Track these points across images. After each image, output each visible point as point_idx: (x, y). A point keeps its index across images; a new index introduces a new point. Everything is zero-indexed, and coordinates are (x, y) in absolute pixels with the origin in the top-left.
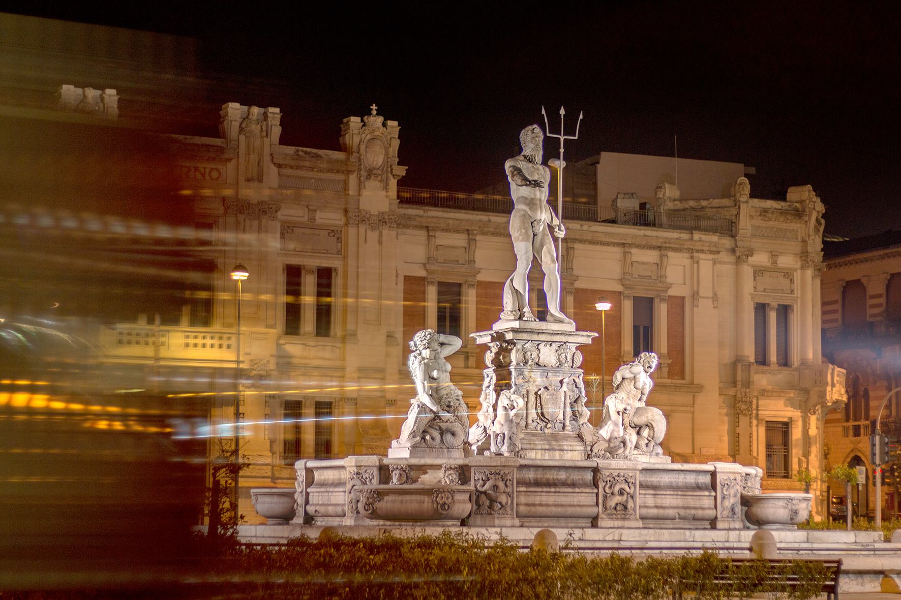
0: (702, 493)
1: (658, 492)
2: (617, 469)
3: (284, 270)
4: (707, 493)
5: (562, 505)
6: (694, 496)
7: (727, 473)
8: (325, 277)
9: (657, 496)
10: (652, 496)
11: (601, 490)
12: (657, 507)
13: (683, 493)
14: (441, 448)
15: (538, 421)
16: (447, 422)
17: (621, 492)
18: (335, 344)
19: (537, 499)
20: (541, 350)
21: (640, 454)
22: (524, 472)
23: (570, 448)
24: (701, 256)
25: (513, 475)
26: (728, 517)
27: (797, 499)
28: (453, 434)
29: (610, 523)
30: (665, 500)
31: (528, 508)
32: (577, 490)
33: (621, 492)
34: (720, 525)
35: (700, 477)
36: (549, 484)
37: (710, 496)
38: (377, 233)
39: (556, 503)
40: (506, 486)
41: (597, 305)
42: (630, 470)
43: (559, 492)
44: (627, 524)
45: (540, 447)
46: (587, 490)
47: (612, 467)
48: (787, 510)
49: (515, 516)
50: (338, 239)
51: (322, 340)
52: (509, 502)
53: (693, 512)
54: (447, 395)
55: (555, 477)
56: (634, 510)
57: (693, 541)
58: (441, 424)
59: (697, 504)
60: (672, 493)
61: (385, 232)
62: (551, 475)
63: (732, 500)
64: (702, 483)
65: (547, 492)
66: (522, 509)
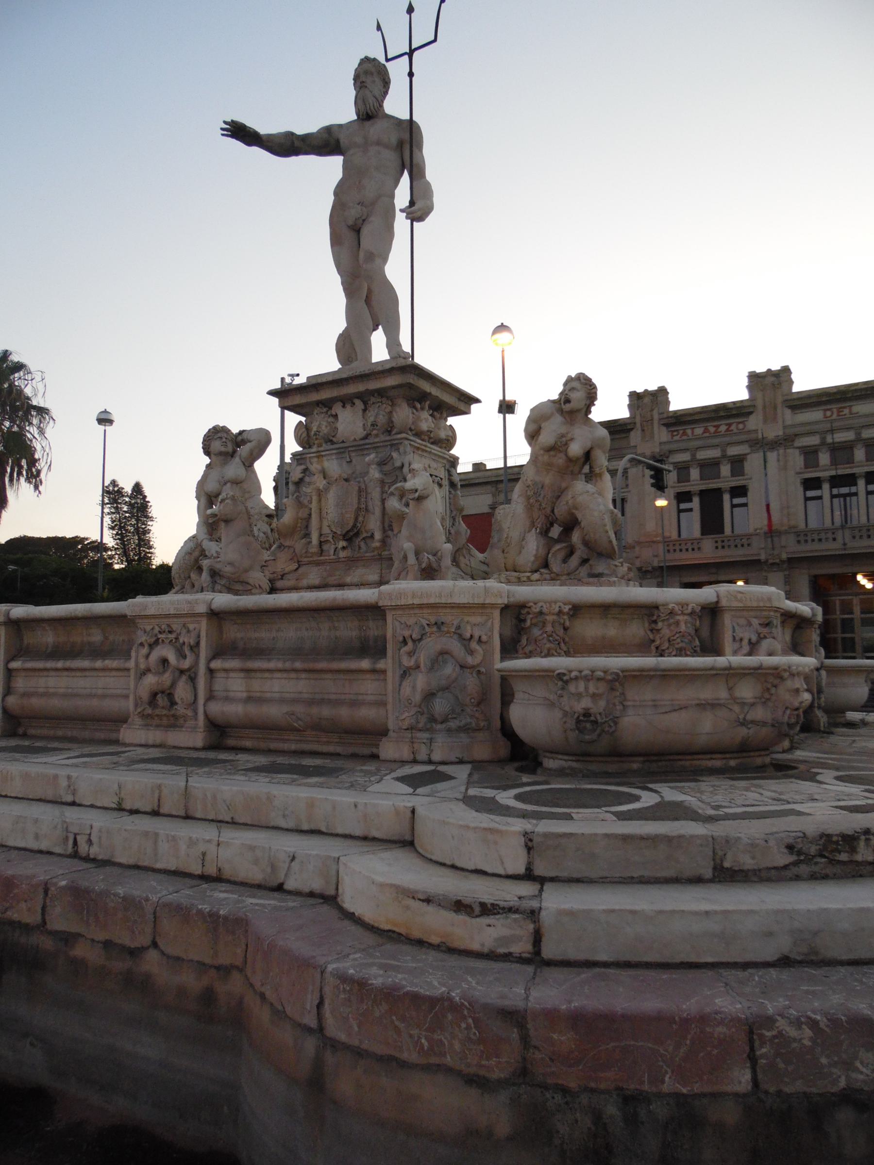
0: (354, 665)
4: (365, 664)
6: (339, 671)
9: (253, 674)
10: (242, 675)
12: (249, 699)
15: (330, 539)
21: (545, 580)
26: (411, 728)
27: (587, 679)
34: (388, 749)
48: (558, 714)
62: (79, 637)
63: (421, 681)
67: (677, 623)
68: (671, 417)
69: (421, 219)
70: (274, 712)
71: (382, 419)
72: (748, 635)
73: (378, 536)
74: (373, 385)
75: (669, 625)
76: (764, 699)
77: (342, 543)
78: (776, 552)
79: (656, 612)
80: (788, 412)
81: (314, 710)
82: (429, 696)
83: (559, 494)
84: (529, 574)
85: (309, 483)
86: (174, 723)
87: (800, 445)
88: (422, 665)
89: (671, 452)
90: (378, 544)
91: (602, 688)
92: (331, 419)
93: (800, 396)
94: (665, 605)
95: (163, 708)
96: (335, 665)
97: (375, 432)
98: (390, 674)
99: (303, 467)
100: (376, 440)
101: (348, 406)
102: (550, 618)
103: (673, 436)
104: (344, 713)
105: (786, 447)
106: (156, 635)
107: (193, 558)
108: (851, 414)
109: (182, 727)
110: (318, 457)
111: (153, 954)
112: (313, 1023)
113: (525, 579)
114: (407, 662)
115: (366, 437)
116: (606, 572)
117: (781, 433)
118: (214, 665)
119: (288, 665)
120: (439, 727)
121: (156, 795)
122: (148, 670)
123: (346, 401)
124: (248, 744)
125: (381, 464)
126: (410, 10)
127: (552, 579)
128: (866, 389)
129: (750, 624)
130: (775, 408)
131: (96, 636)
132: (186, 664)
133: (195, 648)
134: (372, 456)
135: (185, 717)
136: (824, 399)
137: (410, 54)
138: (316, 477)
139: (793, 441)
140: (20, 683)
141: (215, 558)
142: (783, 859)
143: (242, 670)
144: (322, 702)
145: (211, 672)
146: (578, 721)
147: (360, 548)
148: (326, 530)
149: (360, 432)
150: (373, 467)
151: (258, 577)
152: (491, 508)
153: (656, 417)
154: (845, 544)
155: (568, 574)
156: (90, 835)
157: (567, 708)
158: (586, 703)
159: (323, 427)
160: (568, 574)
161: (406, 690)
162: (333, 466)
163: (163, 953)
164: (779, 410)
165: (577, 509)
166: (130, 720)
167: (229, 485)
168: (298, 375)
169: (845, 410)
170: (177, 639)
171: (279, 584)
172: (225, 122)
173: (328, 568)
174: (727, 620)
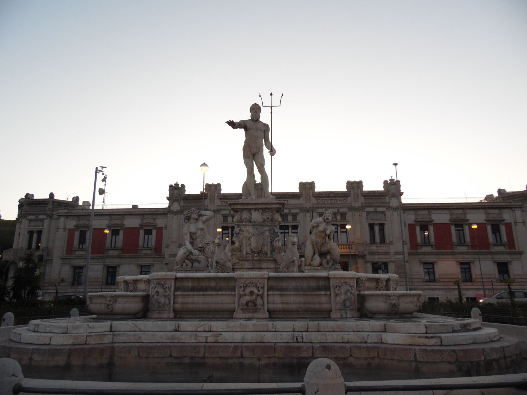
0: (319, 293)
1: (283, 293)
2: (249, 278)
3: (368, 225)
4: (323, 293)
7: (339, 278)
8: (382, 226)
9: (283, 296)
10: (279, 296)
11: (236, 292)
13: (304, 293)
14: (192, 270)
15: (250, 253)
16: (196, 256)
17: (252, 293)
19: (191, 299)
21: (322, 269)
22: (185, 282)
24: (516, 209)
25: (171, 285)
27: (395, 296)
29: (243, 315)
32: (220, 293)
34: (333, 315)
35: (320, 282)
36: (201, 289)
37: (326, 295)
40: (166, 292)
41: (472, 226)
42: (260, 278)
43: (206, 295)
44: (256, 315)
46: (227, 293)
47: (244, 277)
48: (387, 304)
52: (167, 302)
53: (311, 306)
55: (207, 285)
56: (263, 305)
57: (275, 331)
58: (192, 257)
60: (294, 293)
62: (203, 284)
63: (343, 297)
65: (197, 295)
66: (177, 306)
67: (383, 283)
68: (222, 196)
69: (274, 155)
70: (294, 307)
71: (270, 217)
72: (394, 286)
73: (269, 253)
74: (268, 206)
75: (381, 284)
76: (418, 301)
77: (256, 255)
79: (379, 280)
81: (307, 306)
82: (344, 301)
83: (323, 244)
85: (241, 234)
86: (255, 311)
88: (343, 294)
89: (221, 210)
90: (270, 256)
91: (396, 298)
92: (250, 214)
94: (381, 279)
96: (313, 293)
97: (267, 221)
98: (332, 295)
100: (268, 223)
102: (364, 281)
103: (222, 204)
104: (317, 306)
106: (247, 284)
109: (259, 312)
110: (245, 226)
111: (351, 358)
112: (414, 359)
114: (337, 292)
116: (338, 268)
118: (269, 293)
119: (297, 293)
120: (348, 309)
121: (307, 327)
122: (245, 295)
123: (255, 210)
124: (280, 316)
125: (270, 231)
126: (271, 94)
127: (324, 269)
128: (293, 195)
129: (394, 284)
131: (213, 284)
132: (260, 293)
133: (263, 288)
134: (268, 228)
135: (260, 309)
137: (271, 107)
138: (245, 232)
140: (180, 300)
142: (460, 328)
143: (279, 295)
144: (308, 303)
145: (268, 295)
146: (392, 306)
147: (261, 256)
148: (248, 249)
149: (261, 220)
150: (267, 231)
151: (229, 264)
152: (140, 226)
153: (216, 195)
155: (329, 268)
156: (302, 336)
157: (389, 303)
158: (395, 301)
159: (248, 217)
160: (329, 268)
161: (338, 299)
162: (250, 229)
163: (354, 357)
165: (331, 249)
166: (236, 311)
167: (200, 230)
168: (106, 167)
170: (256, 285)
171: (235, 267)
174: (391, 283)
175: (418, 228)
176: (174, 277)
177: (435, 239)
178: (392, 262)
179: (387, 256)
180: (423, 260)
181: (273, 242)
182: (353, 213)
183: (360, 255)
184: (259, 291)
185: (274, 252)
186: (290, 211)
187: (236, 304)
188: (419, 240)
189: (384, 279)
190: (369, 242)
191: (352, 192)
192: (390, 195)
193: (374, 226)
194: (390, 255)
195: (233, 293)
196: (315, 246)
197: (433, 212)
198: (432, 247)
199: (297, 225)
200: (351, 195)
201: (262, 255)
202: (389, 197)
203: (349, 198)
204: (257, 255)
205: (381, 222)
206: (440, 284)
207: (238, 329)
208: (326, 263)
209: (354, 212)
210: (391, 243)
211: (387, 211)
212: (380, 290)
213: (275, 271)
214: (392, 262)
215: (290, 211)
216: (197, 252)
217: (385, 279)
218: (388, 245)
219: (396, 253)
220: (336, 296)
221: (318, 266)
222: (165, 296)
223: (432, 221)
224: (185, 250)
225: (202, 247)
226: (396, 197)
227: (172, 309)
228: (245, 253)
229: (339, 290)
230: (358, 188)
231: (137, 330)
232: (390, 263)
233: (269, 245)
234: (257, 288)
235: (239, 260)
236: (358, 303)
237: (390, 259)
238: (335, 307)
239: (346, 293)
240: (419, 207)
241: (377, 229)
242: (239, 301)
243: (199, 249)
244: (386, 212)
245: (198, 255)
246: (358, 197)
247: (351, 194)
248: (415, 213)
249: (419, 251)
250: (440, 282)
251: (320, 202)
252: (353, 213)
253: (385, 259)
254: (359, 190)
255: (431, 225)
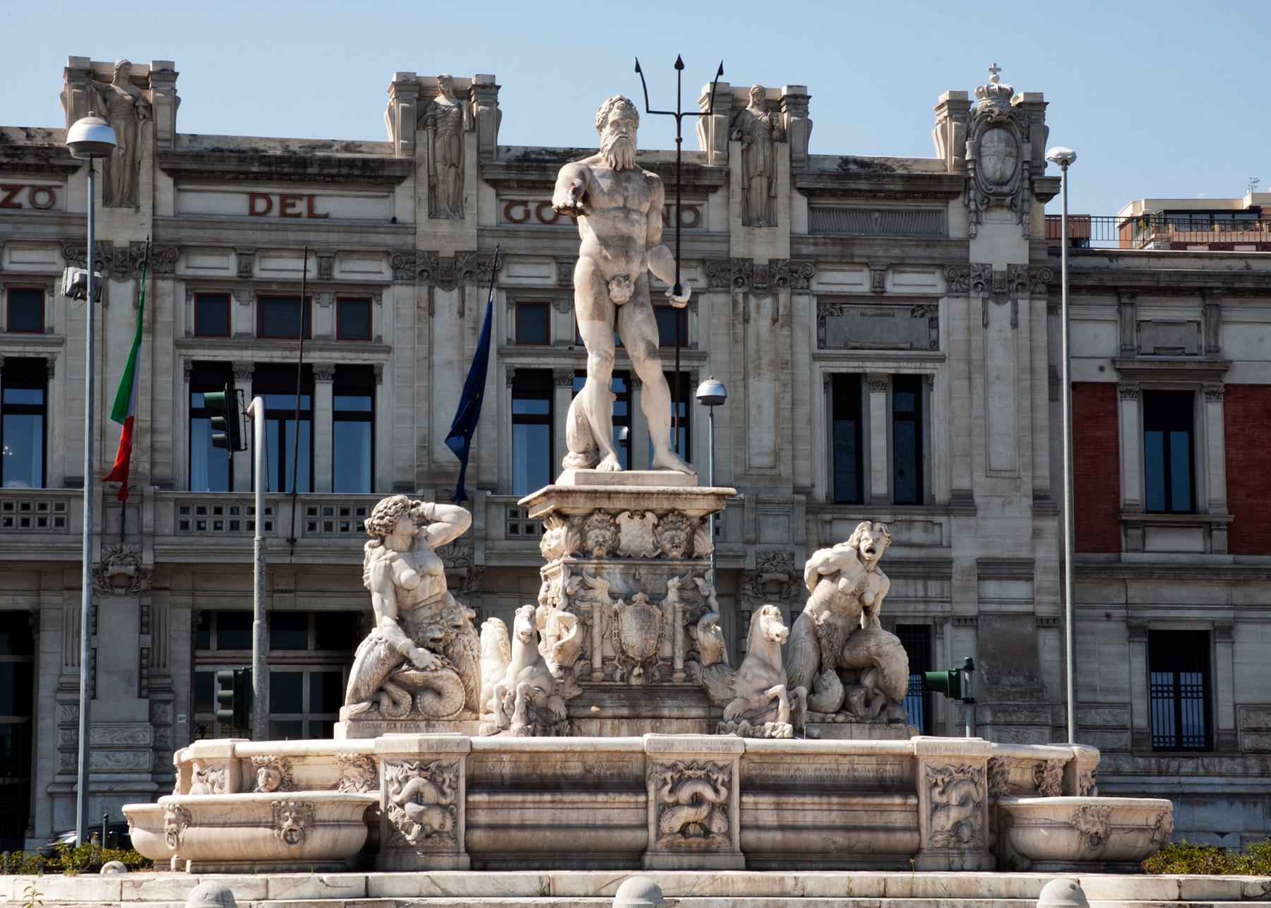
0: (887, 800)
3: (826, 384)
4: (898, 800)
5: (568, 827)
11: (652, 795)
12: (782, 828)
14: (413, 720)
16: (424, 669)
17: (697, 801)
18: (930, 518)
20: (623, 528)
21: (850, 722)
23: (675, 713)
28: (439, 693)
30: (801, 814)
31: (492, 834)
33: (697, 801)
38: (1009, 305)
39: (557, 822)
45: (609, 712)
49: (463, 850)
50: (931, 320)
51: (178, 526)
52: (449, 825)
54: (432, 618)
56: (728, 834)
59: (879, 820)
61: (1023, 304)
63: (955, 814)
64: (892, 779)
66: (479, 836)
73: (679, 664)
78: (126, 549)
80: (166, 183)
82: (958, 826)
84: (834, 716)
87: (190, 272)
92: (612, 528)
93: (197, 147)
95: (695, 835)
99: (580, 578)
101: (637, 518)
104: (882, 839)
105: (156, 275)
107: (386, 668)
108: (311, 214)
113: (830, 720)
115: (658, 557)
117: (144, 235)
118: (745, 799)
121: (882, 885)
122: (677, 804)
126: (679, 65)
127: (857, 722)
128: (350, 163)
130: (135, 167)
133: (728, 785)
136: (255, 169)
137: (679, 117)
139: (173, 261)
141: (432, 671)
142: (1261, 892)
154: (292, 541)
155: (873, 719)
160: (873, 719)
164: (145, 177)
169: (298, 202)
172: (389, 91)
173: (622, 695)
175: (1130, 413)
176: (467, 749)
177: (1231, 484)
178: (962, 621)
179: (934, 588)
180: (1149, 614)
181: (691, 628)
182: (735, 303)
183: (766, 577)
184: (716, 791)
185: (699, 662)
186: (325, 271)
187: (652, 828)
188: (1132, 488)
189: (1060, 760)
190: (821, 491)
191: (736, 165)
192: (972, 194)
193: (865, 388)
194: (949, 578)
195: (642, 798)
196: (824, 641)
197: (1235, 310)
198: (1209, 535)
199: (371, 367)
200: (728, 183)
201: (657, 673)
202: (967, 206)
203: (716, 199)
204: (642, 671)
205: (908, 369)
206: (1237, 765)
207: (707, 890)
208: (863, 700)
209: (740, 297)
210: (963, 503)
211: (949, 293)
212: (1046, 795)
213: (704, 725)
214: (962, 621)
215: (325, 271)
216: (422, 656)
217: (1064, 763)
218: (937, 519)
219: (990, 569)
220: (936, 808)
221: (837, 713)
222: (438, 805)
223: (1226, 366)
224: (381, 650)
225: (440, 640)
226: (1011, 207)
227: (462, 844)
228: (597, 663)
229: (942, 793)
230: (772, 141)
231: (439, 891)
232: (948, 628)
233: (680, 637)
234: (708, 780)
235: (579, 686)
236: (991, 830)
237: (947, 607)
238: (931, 839)
239: (962, 804)
240: (1152, 274)
241: (877, 407)
242: (658, 820)
243: (432, 645)
244: (942, 303)
245: (433, 667)
246: (771, 197)
247: (728, 174)
248: (1120, 312)
249: (1127, 557)
250: (1234, 750)
251: (527, 214)
252: (735, 303)
253: (921, 607)
254: (783, 150)
255: (1212, 394)
